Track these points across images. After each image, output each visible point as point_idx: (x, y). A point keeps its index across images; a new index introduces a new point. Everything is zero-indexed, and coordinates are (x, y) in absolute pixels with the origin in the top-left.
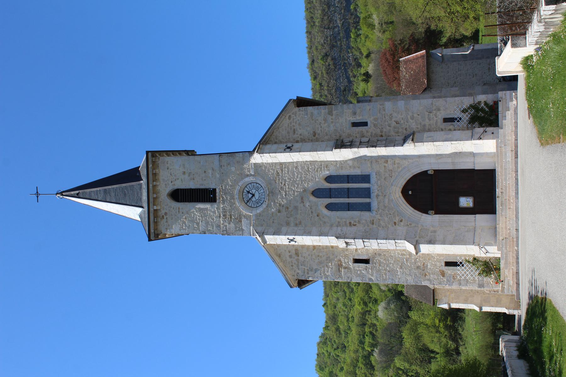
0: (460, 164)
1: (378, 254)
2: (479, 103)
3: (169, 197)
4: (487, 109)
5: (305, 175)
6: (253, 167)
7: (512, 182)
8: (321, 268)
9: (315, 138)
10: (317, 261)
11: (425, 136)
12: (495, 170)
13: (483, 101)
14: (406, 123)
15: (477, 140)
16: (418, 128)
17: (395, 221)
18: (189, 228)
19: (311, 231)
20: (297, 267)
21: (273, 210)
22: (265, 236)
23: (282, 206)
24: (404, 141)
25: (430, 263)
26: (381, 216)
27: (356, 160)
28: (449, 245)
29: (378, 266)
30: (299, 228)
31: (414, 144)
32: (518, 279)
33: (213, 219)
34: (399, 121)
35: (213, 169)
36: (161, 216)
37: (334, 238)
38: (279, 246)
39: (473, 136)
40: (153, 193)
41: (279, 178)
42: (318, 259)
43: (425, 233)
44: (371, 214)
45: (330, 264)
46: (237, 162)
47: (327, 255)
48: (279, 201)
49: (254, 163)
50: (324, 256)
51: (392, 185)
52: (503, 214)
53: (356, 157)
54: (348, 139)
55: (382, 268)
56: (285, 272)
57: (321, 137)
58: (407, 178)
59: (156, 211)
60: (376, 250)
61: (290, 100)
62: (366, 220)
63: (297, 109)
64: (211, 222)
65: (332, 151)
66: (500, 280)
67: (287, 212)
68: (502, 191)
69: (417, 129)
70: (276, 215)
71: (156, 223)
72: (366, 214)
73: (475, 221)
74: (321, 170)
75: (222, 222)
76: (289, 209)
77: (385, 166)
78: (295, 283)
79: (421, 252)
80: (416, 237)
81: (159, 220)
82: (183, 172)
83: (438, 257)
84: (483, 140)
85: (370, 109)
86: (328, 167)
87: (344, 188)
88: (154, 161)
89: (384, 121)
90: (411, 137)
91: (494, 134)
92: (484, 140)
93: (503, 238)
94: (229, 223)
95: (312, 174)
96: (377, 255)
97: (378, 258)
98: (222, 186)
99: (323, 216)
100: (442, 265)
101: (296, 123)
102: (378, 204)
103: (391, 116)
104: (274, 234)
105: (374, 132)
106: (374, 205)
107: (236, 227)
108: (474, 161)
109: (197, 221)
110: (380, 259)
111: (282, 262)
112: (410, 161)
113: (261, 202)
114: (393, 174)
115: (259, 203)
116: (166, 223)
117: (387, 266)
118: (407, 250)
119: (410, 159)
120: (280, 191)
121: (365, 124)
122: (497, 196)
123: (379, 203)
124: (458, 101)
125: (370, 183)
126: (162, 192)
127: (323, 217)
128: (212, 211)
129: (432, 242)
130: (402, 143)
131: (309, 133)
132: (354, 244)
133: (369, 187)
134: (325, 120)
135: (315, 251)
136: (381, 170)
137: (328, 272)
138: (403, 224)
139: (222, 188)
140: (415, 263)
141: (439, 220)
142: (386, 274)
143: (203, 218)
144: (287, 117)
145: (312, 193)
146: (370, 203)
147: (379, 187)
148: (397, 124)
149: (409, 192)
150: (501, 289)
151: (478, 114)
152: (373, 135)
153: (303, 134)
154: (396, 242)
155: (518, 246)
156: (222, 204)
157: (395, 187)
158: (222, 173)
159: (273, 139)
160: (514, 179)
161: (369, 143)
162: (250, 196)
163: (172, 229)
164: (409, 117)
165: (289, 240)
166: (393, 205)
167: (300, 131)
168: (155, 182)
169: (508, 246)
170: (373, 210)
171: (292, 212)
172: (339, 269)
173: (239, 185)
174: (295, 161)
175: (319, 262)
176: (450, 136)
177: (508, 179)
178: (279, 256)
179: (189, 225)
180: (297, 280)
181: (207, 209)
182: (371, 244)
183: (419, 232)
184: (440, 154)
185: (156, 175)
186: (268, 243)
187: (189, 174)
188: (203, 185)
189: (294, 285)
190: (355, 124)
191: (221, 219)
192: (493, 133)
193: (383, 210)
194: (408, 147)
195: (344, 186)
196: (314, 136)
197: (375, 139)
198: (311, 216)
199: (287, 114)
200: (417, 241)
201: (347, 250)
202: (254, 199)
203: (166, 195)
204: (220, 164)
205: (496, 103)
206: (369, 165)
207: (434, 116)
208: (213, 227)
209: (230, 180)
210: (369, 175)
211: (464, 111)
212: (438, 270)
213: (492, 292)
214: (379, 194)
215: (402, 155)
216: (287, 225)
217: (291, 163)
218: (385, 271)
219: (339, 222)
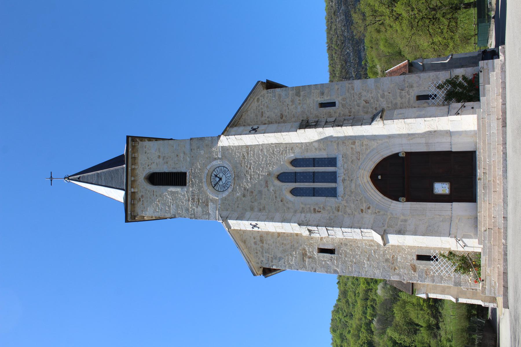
0: (435, 145)
1: (344, 244)
2: (457, 77)
3: (146, 180)
4: (466, 84)
5: (270, 158)
6: (220, 150)
7: (498, 158)
8: (284, 256)
9: (282, 120)
10: (281, 249)
11: (395, 113)
13: (461, 75)
14: (376, 102)
16: (388, 107)
17: (362, 208)
18: (161, 211)
19: (274, 217)
20: (261, 255)
21: (238, 194)
22: (228, 220)
23: (247, 190)
24: (373, 119)
25: (400, 255)
27: (322, 142)
28: (421, 236)
29: (344, 257)
30: (263, 213)
31: (383, 122)
32: (506, 281)
33: (183, 203)
34: (369, 101)
35: (184, 153)
36: (138, 199)
37: (296, 225)
38: (244, 232)
39: (449, 112)
40: (132, 176)
41: (245, 161)
42: (283, 247)
43: (394, 222)
44: (337, 200)
45: (294, 253)
46: (206, 146)
47: (291, 243)
48: (244, 185)
49: (222, 146)
50: (288, 244)
51: (359, 168)
52: (486, 199)
53: (322, 138)
54: (314, 120)
55: (348, 259)
56: (249, 259)
57: (288, 119)
58: (376, 160)
59: (133, 193)
60: (342, 239)
61: (258, 82)
62: (331, 207)
63: (265, 91)
64: (181, 206)
65: (296, 131)
66: (480, 278)
67: (252, 197)
68: (484, 171)
69: (387, 108)
70: (241, 199)
71: (133, 205)
72: (331, 200)
73: (451, 210)
74: (286, 153)
75: (190, 206)
76: (254, 194)
77: (352, 148)
78: (258, 271)
79: (389, 243)
80: (384, 226)
81: (136, 202)
82: (158, 156)
83: (409, 250)
84: (461, 115)
85: (338, 89)
86: (293, 150)
87: (309, 172)
88: (133, 145)
89: (352, 100)
90: (380, 114)
91: (474, 109)
93: (485, 229)
94: (197, 207)
95: (277, 157)
96: (343, 245)
97: (344, 248)
98: (191, 170)
99: (287, 201)
100: (413, 259)
101: (264, 105)
102: (344, 189)
103: (360, 96)
104: (237, 219)
105: (342, 113)
106: (340, 190)
107: (203, 211)
108: (451, 141)
109: (169, 204)
110: (346, 250)
111: (247, 248)
112: (379, 142)
113: (228, 186)
114: (360, 157)
115: (225, 187)
116: (142, 206)
117: (354, 257)
118: (375, 241)
119: (379, 140)
120: (245, 175)
121: (333, 104)
122: (478, 178)
124: (433, 76)
125: (336, 167)
126: (139, 176)
127: (287, 203)
128: (182, 194)
129: (402, 232)
130: (371, 122)
131: (276, 115)
132: (318, 232)
133: (335, 171)
134: (293, 101)
135: (279, 238)
136: (347, 152)
137: (292, 260)
138: (370, 212)
139: (192, 172)
140: (384, 256)
141: (411, 208)
142: (352, 266)
143: (174, 201)
144: (256, 100)
145: (277, 178)
146: (336, 188)
148: (366, 103)
150: (482, 289)
151: (456, 90)
153: (270, 117)
154: (362, 232)
155: (506, 239)
156: (191, 188)
158: (193, 157)
159: (241, 123)
160: (502, 153)
161: (335, 122)
162: (218, 179)
163: (147, 211)
164: (379, 95)
165: (252, 226)
166: (361, 190)
167: (267, 114)
168: (133, 166)
169: (493, 239)
170: (339, 196)
171: (257, 197)
172: (303, 258)
173: (207, 169)
174: (261, 143)
175: (284, 250)
176: (423, 112)
177: (493, 155)
178: (245, 242)
179: (162, 208)
180: (262, 268)
181: (177, 192)
182: (335, 233)
183: (387, 220)
185: (135, 159)
186: (232, 228)
187: (163, 158)
188: (175, 169)
189: (258, 273)
190: (323, 105)
191: (190, 203)
192: (473, 108)
193: (350, 196)
194: (377, 126)
195: (309, 169)
196: (282, 118)
197: (342, 119)
198: (275, 201)
199: (256, 96)
200: (385, 231)
201: (312, 238)
202: (221, 183)
203: (143, 179)
204: (190, 148)
205: (476, 77)
206: (336, 147)
207: (406, 94)
208: (183, 211)
209: (199, 164)
210: (336, 158)
211: (440, 87)
212: (409, 264)
213: (469, 290)
214: (346, 178)
215: (371, 136)
216: (251, 210)
217: (256, 146)
218: (352, 263)
219: (303, 208)
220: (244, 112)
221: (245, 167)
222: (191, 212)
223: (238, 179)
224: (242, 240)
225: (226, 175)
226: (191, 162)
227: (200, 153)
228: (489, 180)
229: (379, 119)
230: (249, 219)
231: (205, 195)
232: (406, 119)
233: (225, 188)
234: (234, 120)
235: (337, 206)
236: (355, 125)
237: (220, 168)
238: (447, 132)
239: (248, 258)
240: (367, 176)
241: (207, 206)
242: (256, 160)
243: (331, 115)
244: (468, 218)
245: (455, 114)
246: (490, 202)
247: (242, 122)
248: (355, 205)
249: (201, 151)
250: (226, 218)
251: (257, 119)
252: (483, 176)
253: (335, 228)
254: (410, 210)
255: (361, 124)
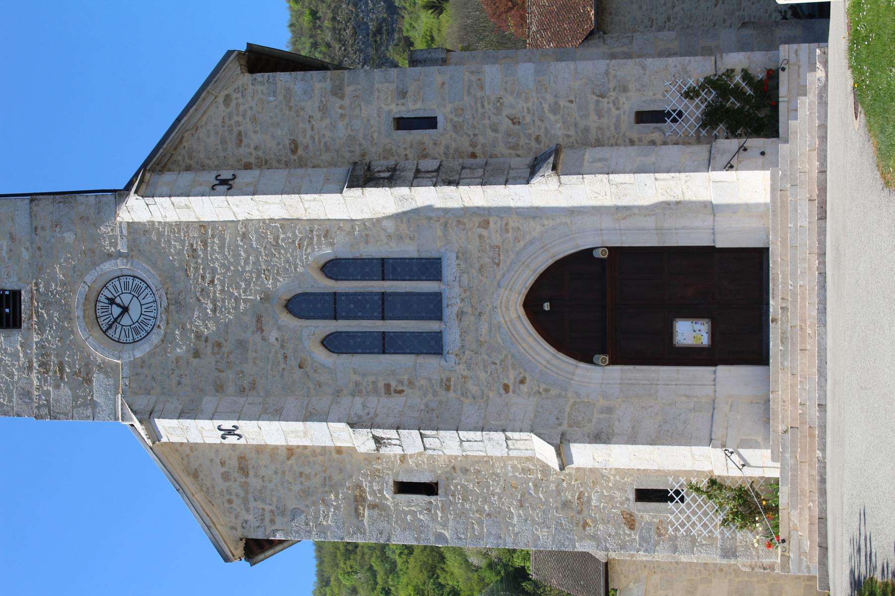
0: (677, 233)
1: (461, 468)
2: (730, 73)
4: (749, 91)
5: (266, 255)
6: (125, 232)
7: (808, 282)
8: (307, 506)
9: (295, 157)
10: (297, 488)
11: (587, 157)
12: (767, 249)
13: (738, 69)
14: (538, 123)
15: (721, 170)
16: (568, 136)
17: (506, 381)
19: (282, 408)
20: (242, 506)
21: (178, 350)
22: (156, 420)
23: (203, 339)
24: (533, 170)
25: (597, 492)
26: (469, 368)
27: (404, 220)
28: (647, 444)
29: (460, 501)
30: (250, 399)
31: (559, 179)
32: (823, 535)
33: (11, 375)
34: (521, 118)
35: (12, 238)
37: (343, 425)
38: (193, 447)
39: (711, 160)
41: (196, 263)
42: (301, 483)
44: (443, 363)
45: (332, 496)
47: (325, 471)
48: (197, 327)
49: (128, 223)
50: (316, 475)
51: (499, 285)
52: (786, 364)
53: (405, 209)
54: (385, 163)
55: (471, 506)
57: (311, 154)
58: (539, 267)
60: (456, 457)
61: (230, 53)
62: (430, 380)
63: (248, 77)
65: (341, 193)
66: (778, 537)
67: (218, 357)
68: (784, 305)
69: (565, 138)
70: (188, 363)
72: (430, 363)
73: (714, 383)
74: (311, 243)
75: (36, 383)
76: (223, 349)
78: (236, 549)
79: (573, 463)
80: (560, 425)
83: (618, 478)
84: (737, 170)
85: (443, 84)
86: (329, 236)
87: (371, 294)
89: (479, 115)
91: (767, 156)
92: (739, 172)
94: (57, 387)
95: (286, 254)
96: (458, 471)
97: (460, 480)
98: (37, 284)
99: (316, 367)
100: (627, 499)
101: (244, 116)
102: (461, 336)
103: (498, 104)
105: (454, 145)
106: (452, 339)
107: (75, 398)
108: (714, 226)
110: (466, 483)
111: (202, 491)
112: (546, 222)
113: (147, 328)
114: (501, 258)
115: (140, 332)
117: (485, 500)
118: (538, 460)
119: (548, 218)
120: (199, 300)
121: (430, 123)
122: (771, 318)
123: (465, 332)
124: (676, 66)
125: (440, 280)
127: (315, 371)
128: (9, 351)
129: (604, 436)
130: (528, 176)
131: (279, 144)
132: (398, 442)
134: (324, 109)
135: (292, 461)
136: (469, 247)
137: (326, 516)
138: (526, 390)
139: (37, 290)
140: (559, 494)
141: (621, 379)
142: (480, 523)
144: (221, 99)
145: (286, 306)
146: (441, 332)
147: (465, 291)
148: (514, 123)
149: (542, 306)
150: (781, 560)
151: (726, 103)
152: (452, 152)
153: (263, 147)
154: (507, 439)
155: (823, 450)
156: (38, 334)
157: (507, 292)
158: (39, 249)
159: (180, 158)
160: (817, 273)
162: (116, 311)
164: (546, 106)
166: (502, 339)
167: (255, 139)
169: (799, 449)
170: (448, 353)
171: (232, 356)
172: (356, 509)
174: (241, 217)
175: (304, 491)
176: (652, 159)
177: (801, 272)
178: (195, 475)
180: (244, 541)
182: (442, 443)
183: (568, 410)
184: (625, 207)
186: (164, 439)
189: (235, 553)
190: (403, 124)
191: (34, 375)
192: (763, 153)
193: (476, 353)
194: (544, 187)
195: (372, 287)
196: (294, 151)
197: (456, 164)
198: (283, 366)
199: (221, 90)
200: (563, 434)
201: (379, 458)
202: (126, 320)
204: (31, 224)
205: (773, 76)
206: (440, 233)
207: (611, 105)
211: (690, 94)
212: (619, 512)
213: (757, 570)
214: (465, 310)
215: (528, 208)
216: (217, 391)
217: (229, 224)
218: (480, 514)
219: (357, 384)
220: (187, 131)
221: (198, 278)
222: (40, 399)
223: (177, 312)
224: (187, 471)
225: (141, 298)
226: (35, 263)
227: (64, 240)
228: (792, 325)
229: (550, 171)
230: (213, 415)
231: (81, 352)
232: (612, 173)
233: (137, 333)
234: (161, 151)
235: (443, 377)
236: (491, 184)
237: (123, 280)
238: (706, 206)
239: (208, 516)
240: (517, 303)
241: (86, 383)
242: (228, 261)
243: (425, 149)
244: (752, 402)
245: (724, 168)
246: (794, 373)
247: (183, 156)
248: (489, 374)
249: (65, 235)
250: (150, 415)
251: (225, 150)
252: (782, 316)
253: (441, 432)
254: (621, 384)
255: (505, 179)
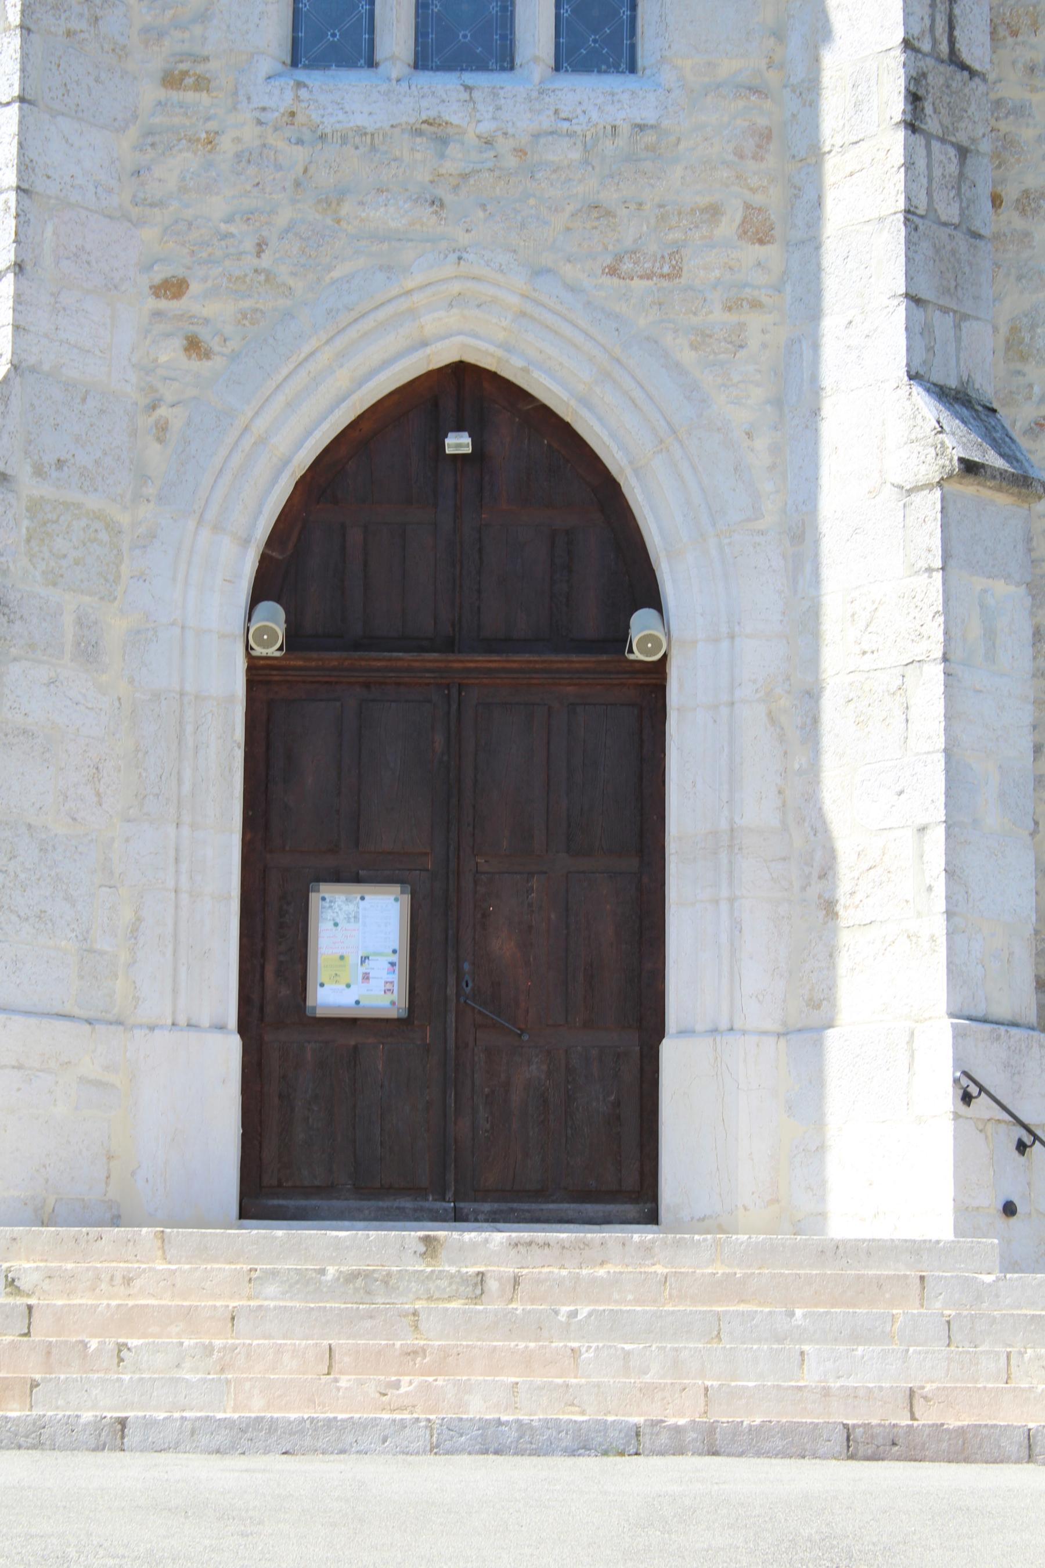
0: (716, 902)
11: (1001, 588)
12: (652, 1218)
15: (957, 1061)
17: (195, 287)
26: (243, 158)
31: (929, 486)
39: (987, 1027)
43: (77, 562)
44: (265, 66)
51: (539, 272)
52: (271, 1289)
58: (600, 419)
68: (492, 1285)
73: (182, 1020)
77: (714, 212)
80: (39, 471)
84: (957, 1116)
90: (999, 463)
92: (947, 1126)
93: (23, 1284)
102: (362, 132)
108: (744, 1032)
112: (761, 443)
114: (635, 282)
123: (373, 148)
125: (557, 68)
130: (936, 377)
133: (518, 61)
138: (163, 358)
146: (371, 63)
147: (520, 152)
149: (459, 429)
152: (1004, 126)
157: (514, 300)
161: (952, 68)
170: (299, 85)
177: (627, 1354)
183: (93, 502)
184: (815, 721)
192: (1009, 1209)
193: (297, 184)
210: (632, 68)
228: (423, 1316)
229: (959, 453)
232: (947, 674)
235: (213, 65)
236: (910, 244)
238: (818, 1006)
240: (476, 336)
243: (1015, 34)
244: (110, 1158)
245: (965, 1074)
246: (240, 1323)
248: (223, 227)
252: (452, 1276)
253: (17, 42)
254: (182, 694)
255: (923, 295)
